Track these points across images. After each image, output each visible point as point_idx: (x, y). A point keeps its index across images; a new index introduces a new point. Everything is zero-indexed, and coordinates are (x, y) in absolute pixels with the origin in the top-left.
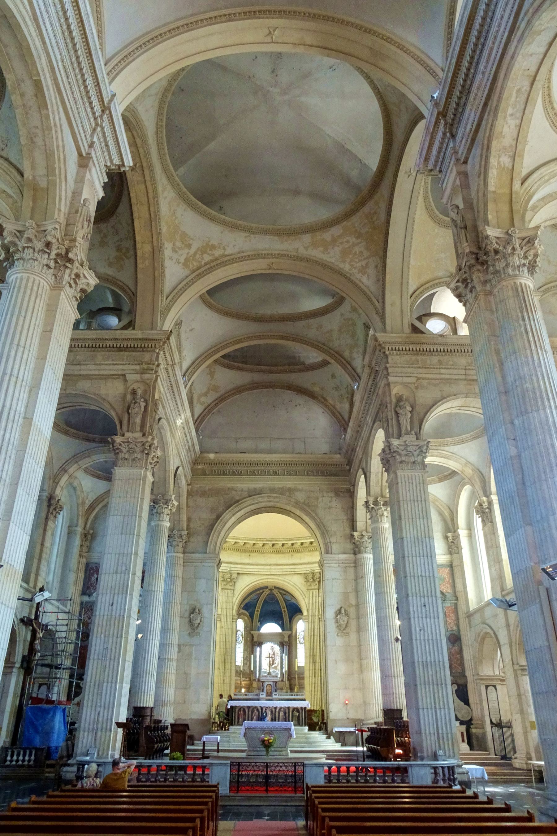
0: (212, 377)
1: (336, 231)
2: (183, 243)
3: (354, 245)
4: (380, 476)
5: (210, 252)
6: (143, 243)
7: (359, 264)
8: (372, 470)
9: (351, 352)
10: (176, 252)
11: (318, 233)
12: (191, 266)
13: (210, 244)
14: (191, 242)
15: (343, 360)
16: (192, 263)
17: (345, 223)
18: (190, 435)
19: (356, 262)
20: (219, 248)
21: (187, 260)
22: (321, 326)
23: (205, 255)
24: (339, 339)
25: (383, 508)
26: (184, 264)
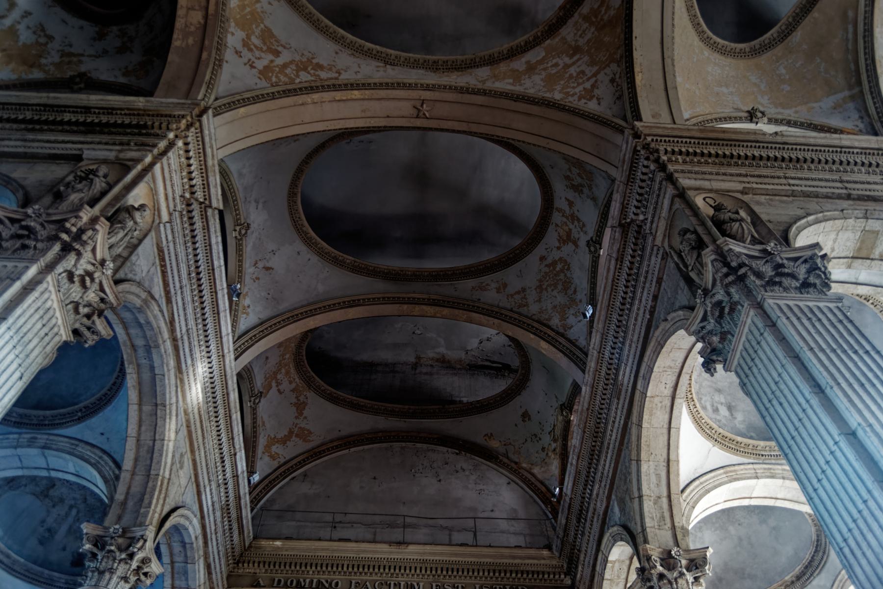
0: (300, 414)
1: (534, 55)
2: (265, 43)
3: (566, 66)
4: (665, 505)
5: (312, 72)
6: (188, 9)
7: (581, 88)
8: (645, 490)
9: (563, 318)
10: (250, 50)
11: (502, 65)
12: (274, 79)
13: (314, 61)
14: (280, 49)
15: (549, 332)
16: (277, 77)
17: (548, 42)
18: (234, 465)
19: (574, 88)
20: (330, 69)
21: (266, 68)
22: (505, 285)
23: (302, 74)
24: (539, 301)
25: (690, 577)
26: (260, 72)
